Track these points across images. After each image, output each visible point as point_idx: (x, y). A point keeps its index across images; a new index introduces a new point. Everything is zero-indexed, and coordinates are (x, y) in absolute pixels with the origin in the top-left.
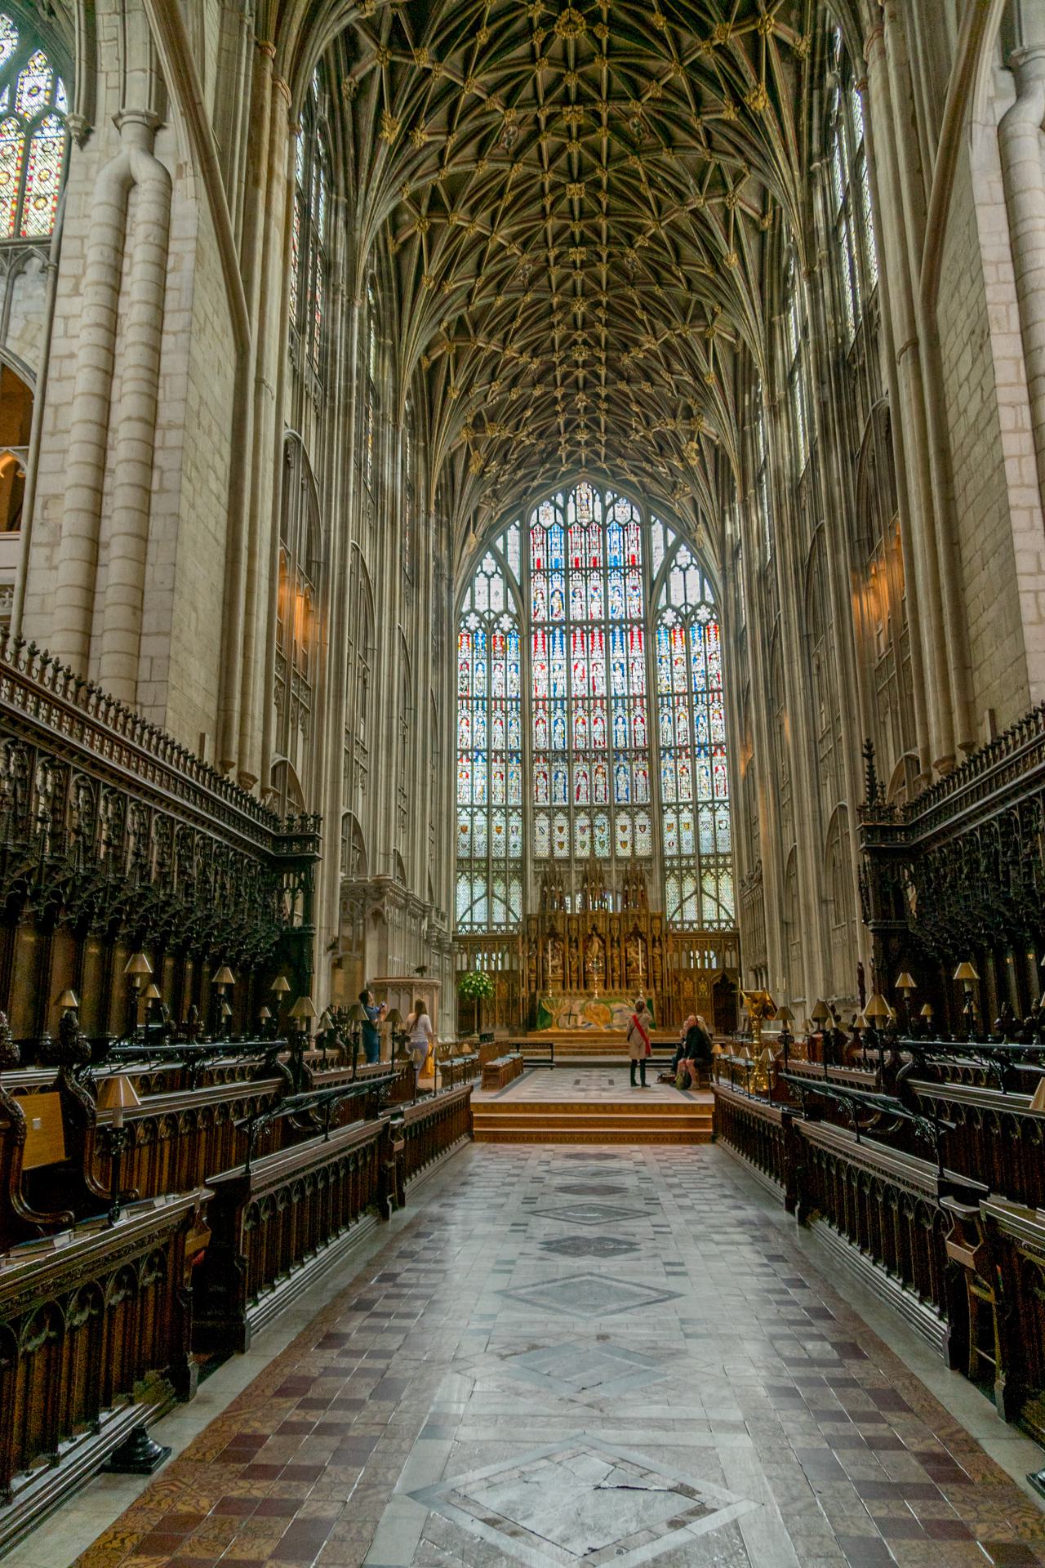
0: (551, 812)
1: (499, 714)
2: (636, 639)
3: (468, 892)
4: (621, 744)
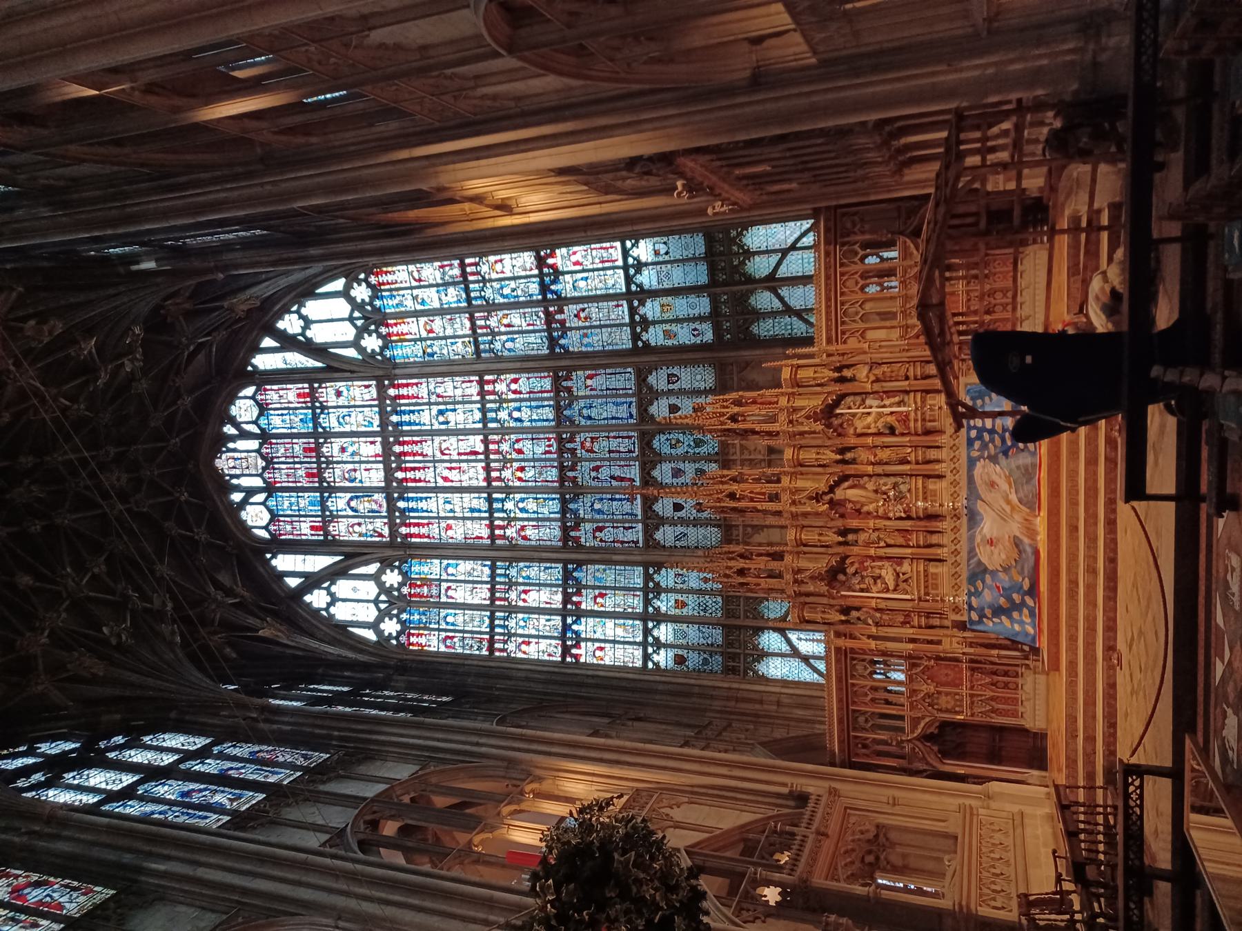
0: (652, 521)
1: (513, 595)
2: (404, 391)
3: (777, 661)
4: (548, 413)
